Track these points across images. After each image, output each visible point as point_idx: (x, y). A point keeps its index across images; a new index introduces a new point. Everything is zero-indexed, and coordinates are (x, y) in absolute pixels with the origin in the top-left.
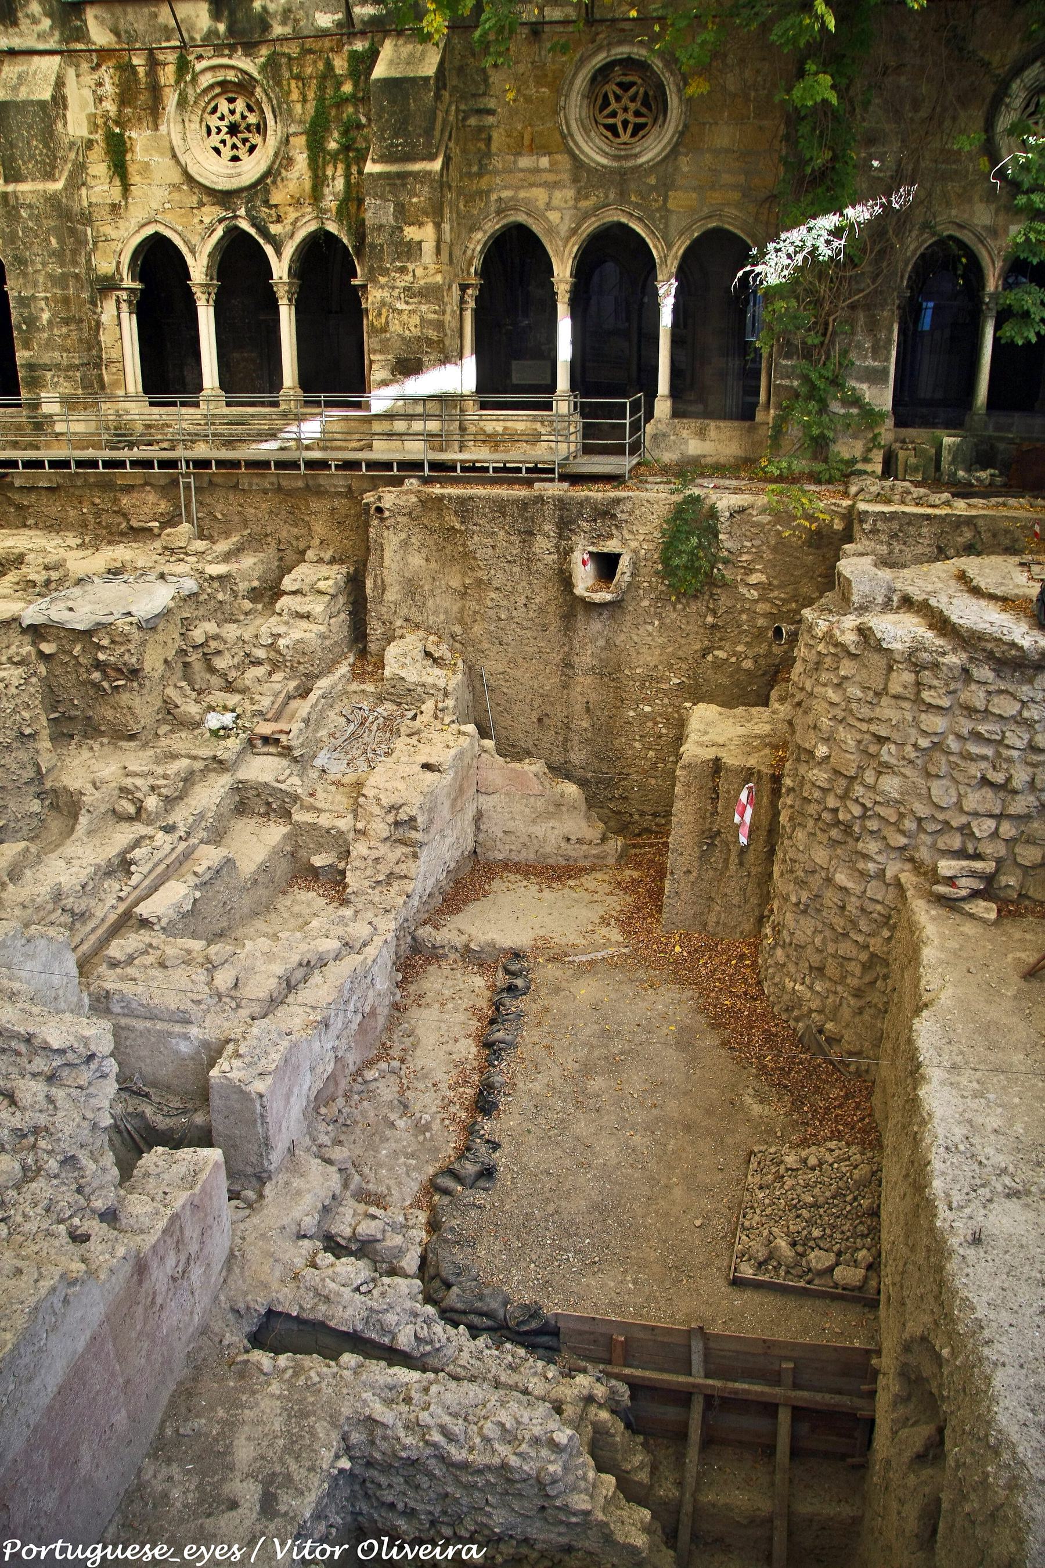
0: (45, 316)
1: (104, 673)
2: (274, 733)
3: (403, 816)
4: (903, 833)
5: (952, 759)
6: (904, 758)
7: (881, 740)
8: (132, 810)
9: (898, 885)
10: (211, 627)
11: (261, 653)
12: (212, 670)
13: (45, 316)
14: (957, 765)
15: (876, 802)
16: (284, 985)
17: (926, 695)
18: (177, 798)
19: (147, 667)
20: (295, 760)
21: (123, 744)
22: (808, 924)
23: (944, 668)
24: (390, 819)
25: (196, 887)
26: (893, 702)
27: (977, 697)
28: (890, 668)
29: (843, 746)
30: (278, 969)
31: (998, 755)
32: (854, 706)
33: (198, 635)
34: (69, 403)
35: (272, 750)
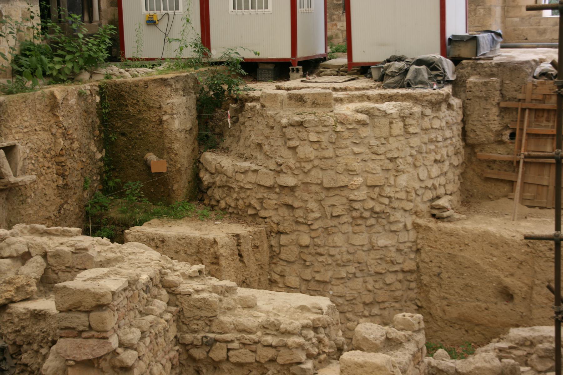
4: (411, 201)
5: (424, 155)
6: (407, 163)
7: (392, 160)
9: (416, 226)
14: (426, 157)
15: (397, 192)
17: (411, 130)
22: (358, 284)
23: (416, 114)
26: (394, 139)
27: (426, 123)
28: (391, 123)
29: (374, 172)
31: (436, 146)
32: (375, 149)
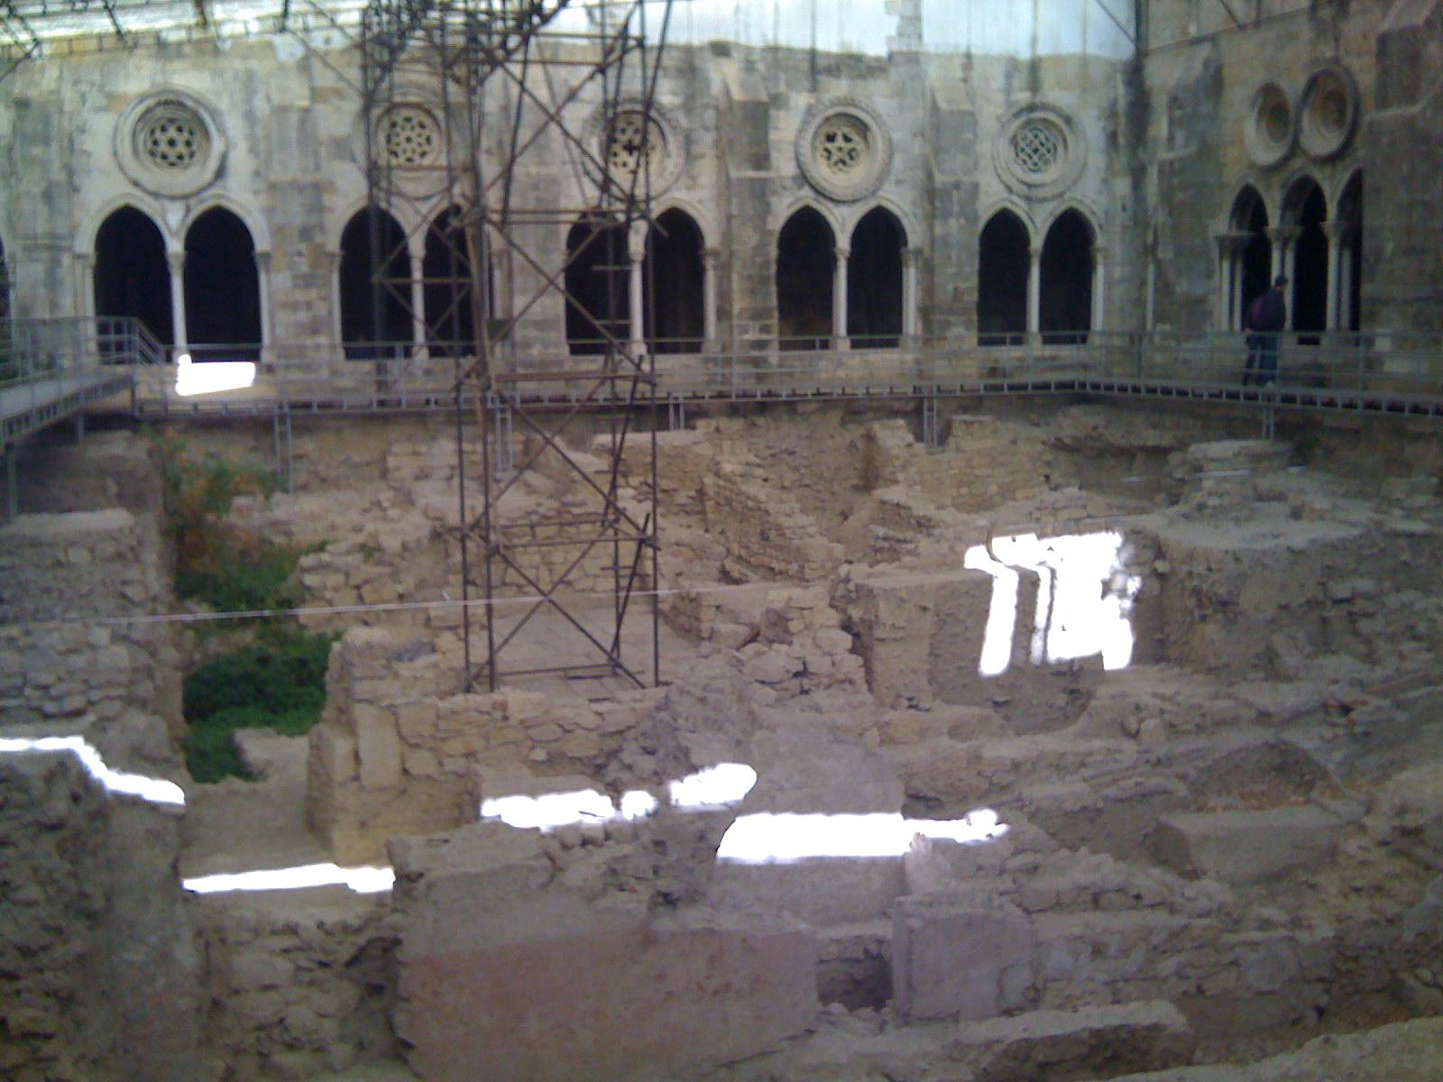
0: (1390, 247)
1: (1200, 600)
2: (1355, 702)
3: (1411, 821)
8: (1133, 726)
10: (1365, 585)
11: (1422, 627)
12: (1356, 633)
13: (1390, 247)
16: (1087, 897)
18: (1189, 732)
19: (1246, 601)
20: (1354, 737)
21: (1199, 678)
24: (1396, 822)
25: (1106, 799)
30: (1085, 879)
33: (1341, 590)
34: (1400, 340)
35: (1342, 720)
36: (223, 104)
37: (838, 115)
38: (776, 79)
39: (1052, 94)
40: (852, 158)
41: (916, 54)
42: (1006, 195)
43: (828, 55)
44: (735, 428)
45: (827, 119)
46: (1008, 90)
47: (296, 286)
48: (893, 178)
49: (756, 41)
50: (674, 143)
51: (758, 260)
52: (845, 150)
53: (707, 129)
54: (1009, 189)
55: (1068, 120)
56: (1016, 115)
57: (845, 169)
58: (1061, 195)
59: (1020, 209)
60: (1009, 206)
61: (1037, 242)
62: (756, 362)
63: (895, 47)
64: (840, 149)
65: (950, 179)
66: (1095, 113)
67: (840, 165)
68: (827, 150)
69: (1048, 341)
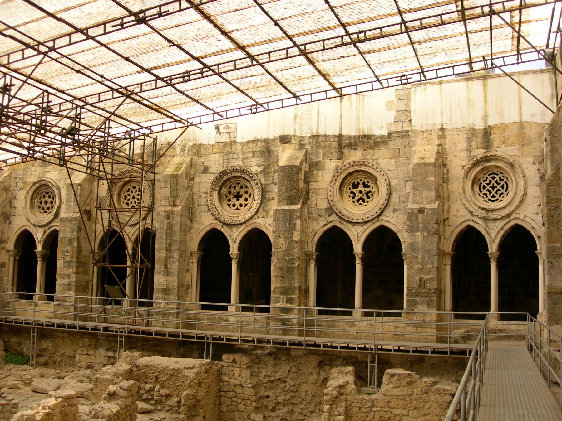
36: (61, 185)
37: (358, 171)
38: (317, 153)
39: (499, 150)
40: (368, 197)
41: (408, 131)
42: (470, 217)
43: (350, 137)
44: (245, 361)
45: (351, 174)
46: (469, 150)
47: (65, 266)
48: (391, 208)
49: (307, 133)
50: (256, 192)
51: (287, 258)
52: (364, 192)
53: (276, 184)
54: (471, 213)
55: (512, 165)
56: (475, 165)
57: (365, 204)
58: (508, 215)
59: (480, 226)
60: (472, 224)
61: (493, 248)
62: (284, 322)
63: (393, 129)
64: (361, 192)
65: (418, 206)
66: (531, 160)
67: (361, 202)
68: (352, 193)
69: (503, 318)
